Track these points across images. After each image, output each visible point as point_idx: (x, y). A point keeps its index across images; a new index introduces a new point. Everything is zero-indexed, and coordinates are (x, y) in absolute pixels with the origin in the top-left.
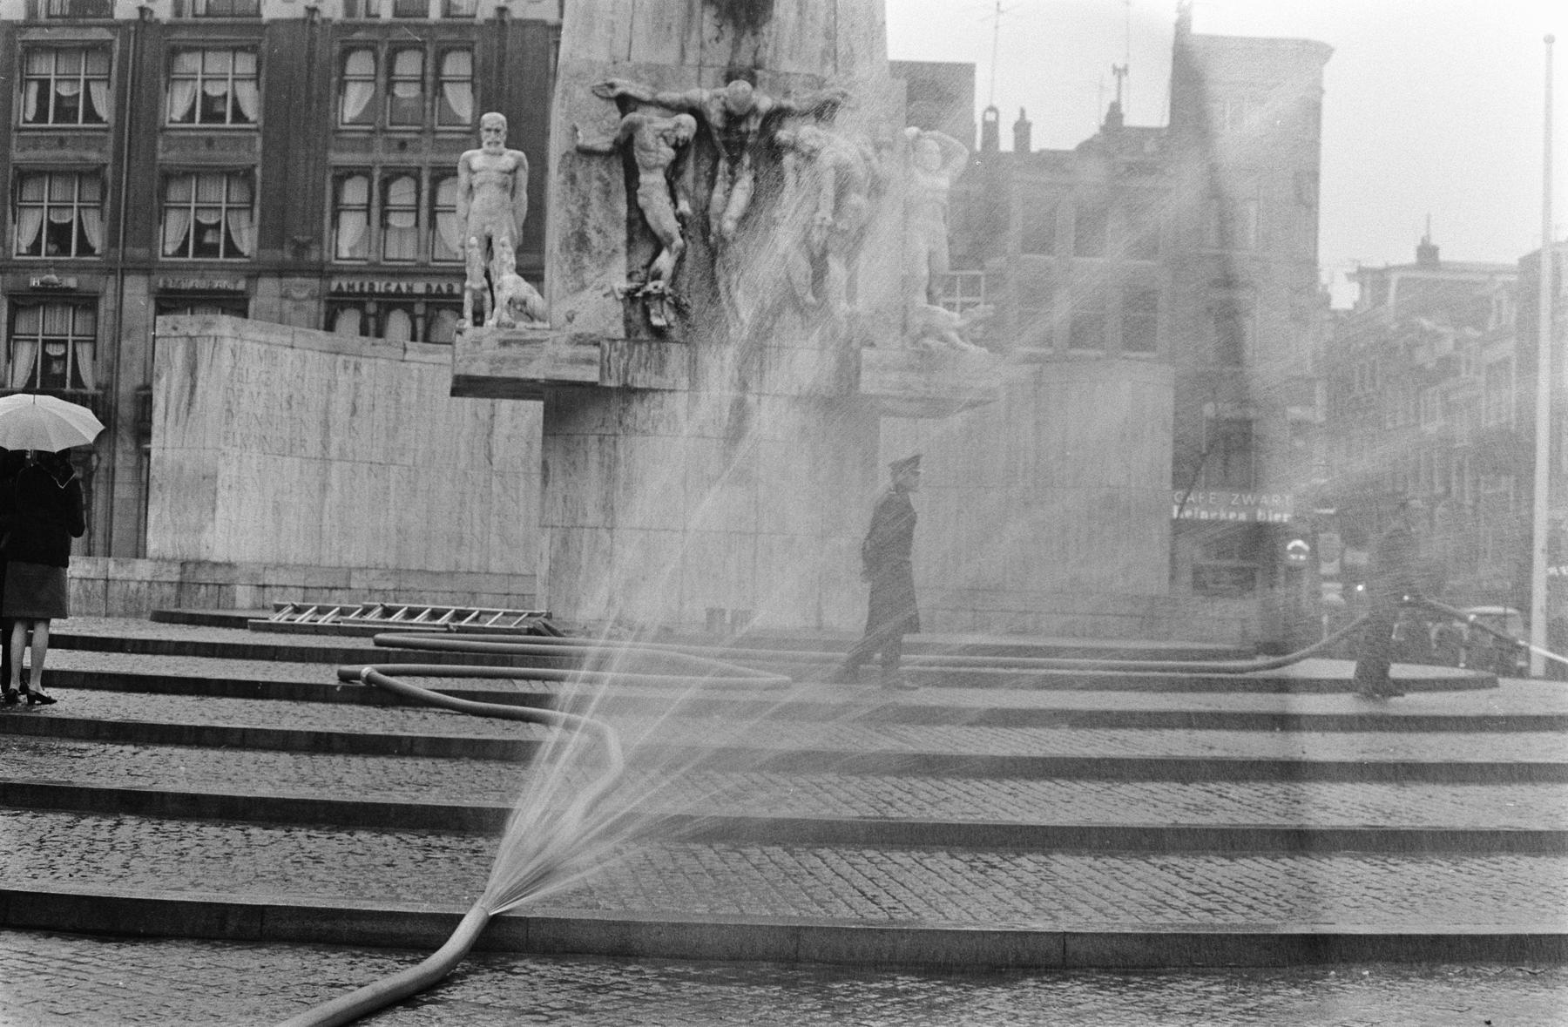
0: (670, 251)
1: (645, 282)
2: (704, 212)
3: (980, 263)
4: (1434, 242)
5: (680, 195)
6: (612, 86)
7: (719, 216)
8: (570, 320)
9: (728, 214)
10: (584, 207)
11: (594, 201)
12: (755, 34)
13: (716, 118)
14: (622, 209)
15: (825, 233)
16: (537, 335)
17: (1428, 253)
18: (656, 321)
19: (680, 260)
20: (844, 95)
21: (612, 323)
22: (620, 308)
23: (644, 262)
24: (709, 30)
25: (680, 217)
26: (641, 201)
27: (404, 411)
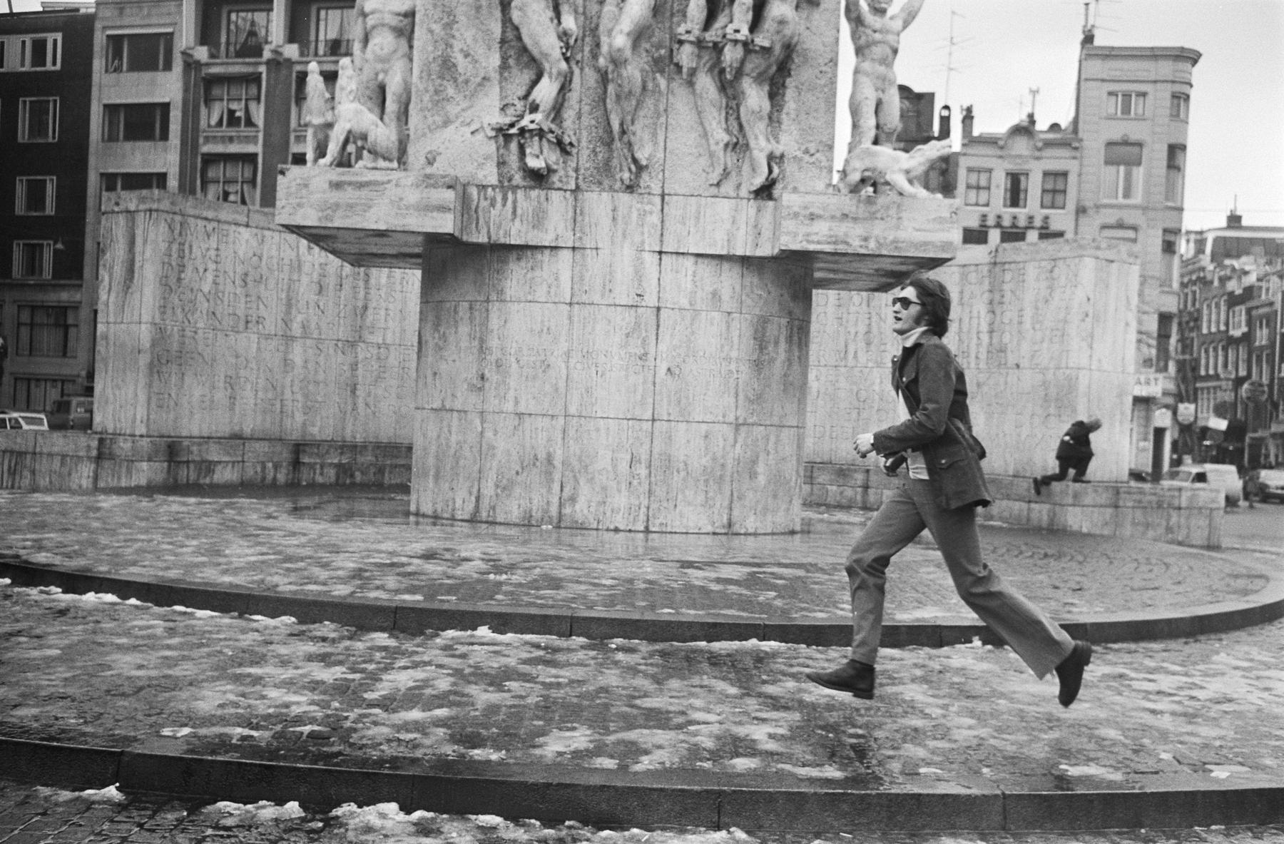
0: (550, 77)
1: (522, 117)
2: (592, 30)
4: (1238, 213)
7: (610, 32)
9: (618, 28)
10: (448, 26)
11: (462, 19)
14: (497, 29)
15: (740, 49)
16: (377, 176)
17: (1234, 221)
18: (533, 163)
19: (564, 89)
21: (481, 166)
22: (492, 147)
23: (521, 92)
25: (564, 35)
26: (516, 15)
27: (372, 292)
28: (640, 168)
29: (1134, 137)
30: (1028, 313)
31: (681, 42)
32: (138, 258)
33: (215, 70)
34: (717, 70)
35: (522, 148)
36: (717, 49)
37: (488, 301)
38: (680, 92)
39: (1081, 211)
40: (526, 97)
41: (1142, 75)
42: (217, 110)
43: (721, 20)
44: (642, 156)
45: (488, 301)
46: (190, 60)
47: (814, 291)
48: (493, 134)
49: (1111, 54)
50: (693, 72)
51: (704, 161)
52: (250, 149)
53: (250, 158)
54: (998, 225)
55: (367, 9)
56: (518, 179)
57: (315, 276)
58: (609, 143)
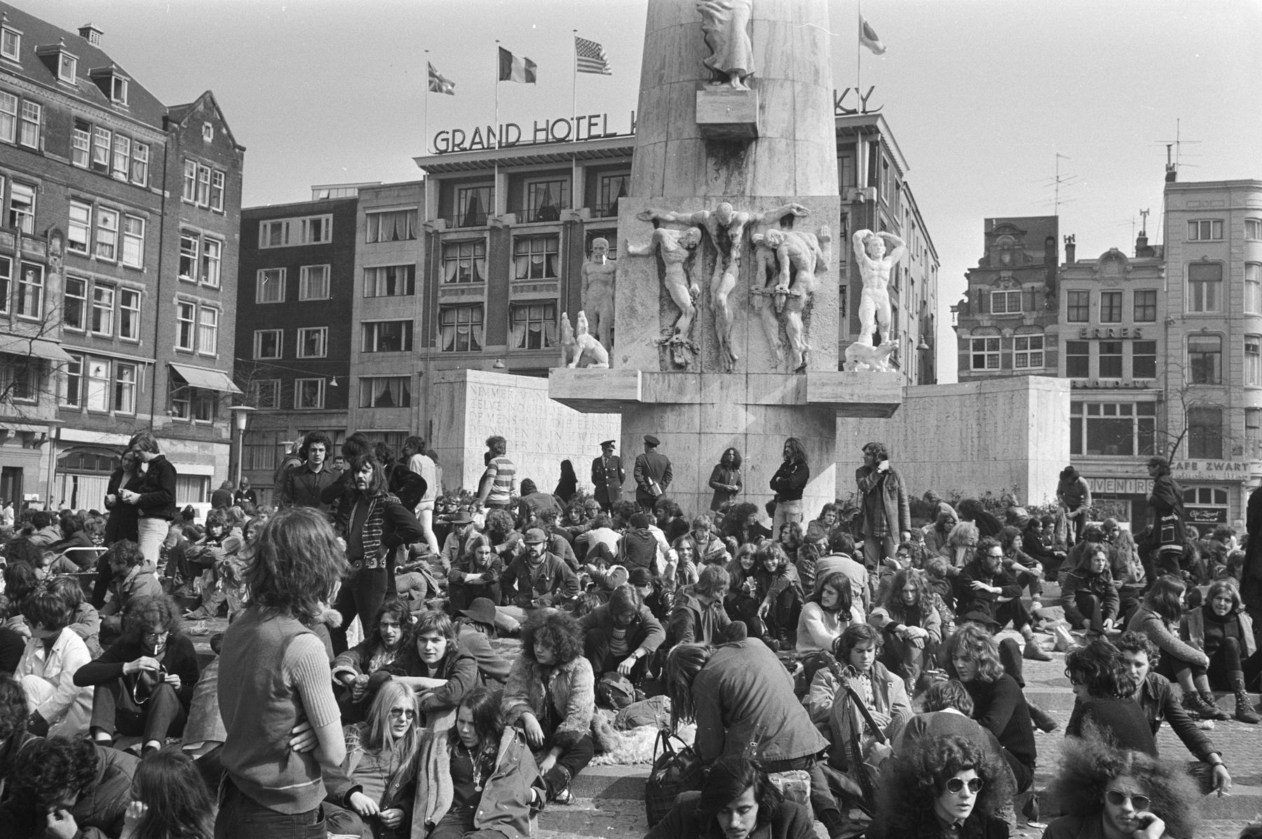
1: (671, 336)
2: (707, 289)
3: (1042, 329)
5: (692, 279)
6: (649, 213)
8: (625, 361)
10: (633, 290)
12: (740, 173)
13: (713, 231)
14: (657, 291)
18: (678, 360)
20: (798, 209)
22: (657, 351)
23: (671, 323)
25: (693, 294)
26: (667, 284)
28: (734, 360)
29: (1211, 258)
30: (1000, 424)
32: (456, 410)
33: (449, 237)
34: (774, 308)
35: (672, 353)
38: (755, 320)
39: (1167, 324)
41: (1216, 205)
42: (452, 268)
43: (774, 282)
46: (430, 230)
47: (839, 420)
49: (1189, 188)
50: (760, 309)
51: (767, 356)
52: (478, 299)
53: (478, 306)
54: (1096, 338)
55: (588, 271)
56: (670, 369)
57: (555, 416)
58: (718, 348)
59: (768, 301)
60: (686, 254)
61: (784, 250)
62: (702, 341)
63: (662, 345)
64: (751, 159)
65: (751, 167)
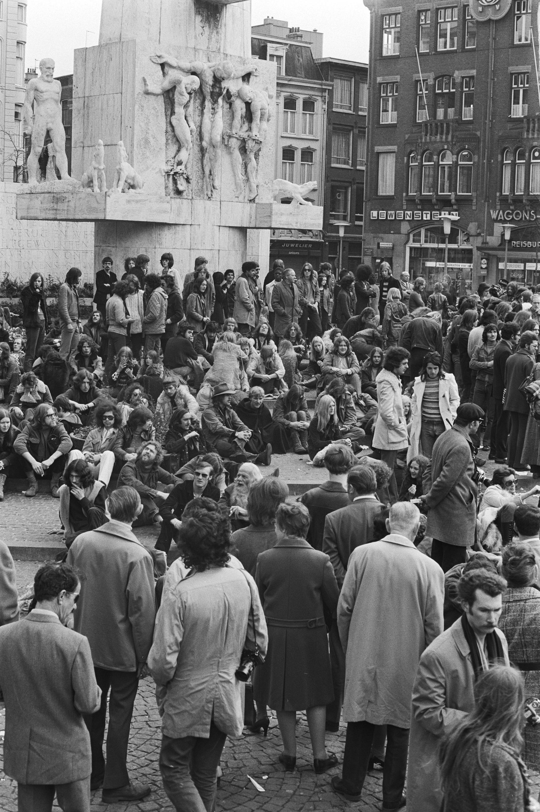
0: (187, 150)
6: (159, 57)
10: (147, 124)
18: (181, 188)
20: (256, 70)
22: (162, 180)
23: (173, 155)
24: (199, 30)
31: (230, 137)
34: (243, 150)
35: (175, 182)
36: (244, 141)
37: (155, 248)
40: (175, 157)
44: (217, 183)
45: (155, 248)
48: (164, 174)
51: (233, 187)
56: (172, 195)
59: (239, 143)
60: (188, 96)
61: (256, 106)
62: (193, 171)
63: (168, 174)
64: (223, 21)
65: (223, 27)
